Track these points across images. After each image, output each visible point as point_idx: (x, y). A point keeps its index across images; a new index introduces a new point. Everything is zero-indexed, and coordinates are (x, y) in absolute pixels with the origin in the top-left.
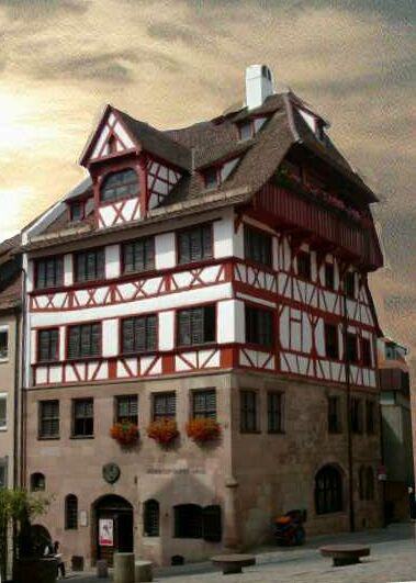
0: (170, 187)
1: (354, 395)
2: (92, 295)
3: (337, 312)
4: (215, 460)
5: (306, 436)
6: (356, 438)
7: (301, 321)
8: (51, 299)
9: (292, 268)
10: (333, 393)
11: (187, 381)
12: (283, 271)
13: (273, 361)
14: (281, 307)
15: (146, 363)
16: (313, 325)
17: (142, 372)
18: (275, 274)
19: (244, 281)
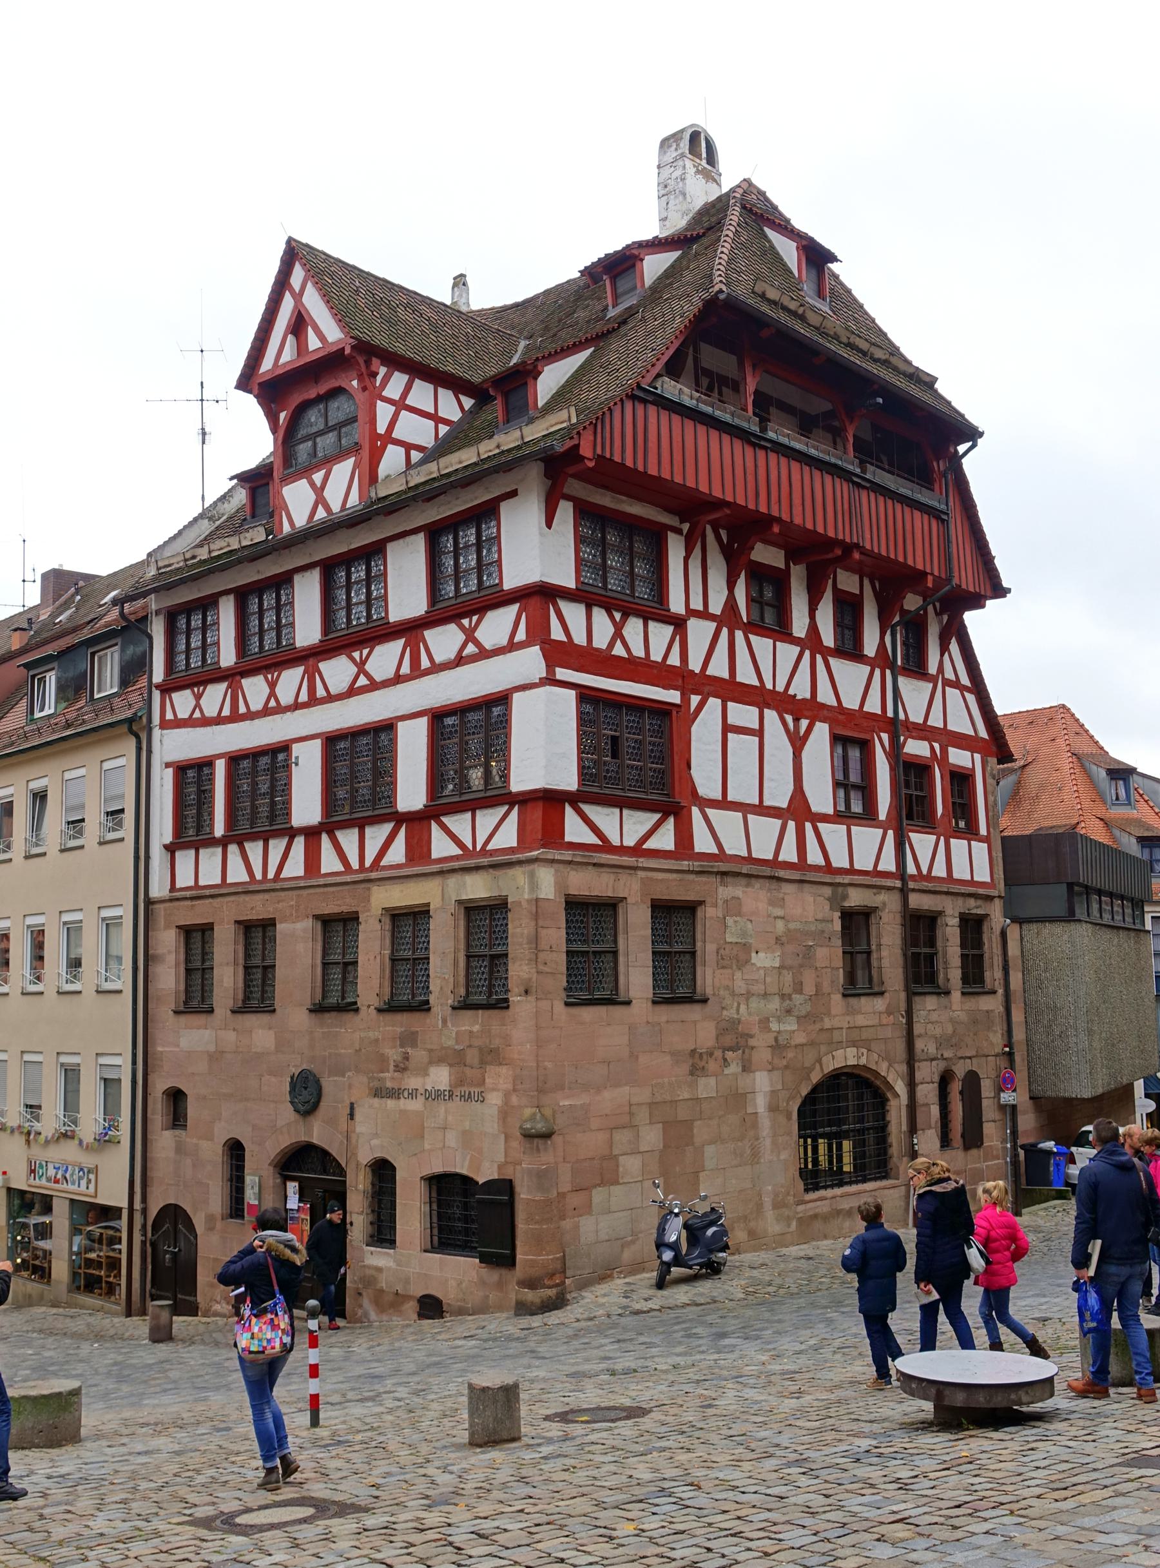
0: (443, 429)
1: (916, 901)
2: (272, 685)
3: (873, 706)
4: (504, 1070)
5: (774, 1004)
6: (927, 1005)
7: (760, 733)
8: (198, 697)
9: (731, 604)
10: (856, 899)
11: (452, 881)
12: (705, 615)
14: (695, 700)
15: (376, 835)
16: (798, 742)
17: (368, 864)
18: (679, 624)
19: (580, 639)
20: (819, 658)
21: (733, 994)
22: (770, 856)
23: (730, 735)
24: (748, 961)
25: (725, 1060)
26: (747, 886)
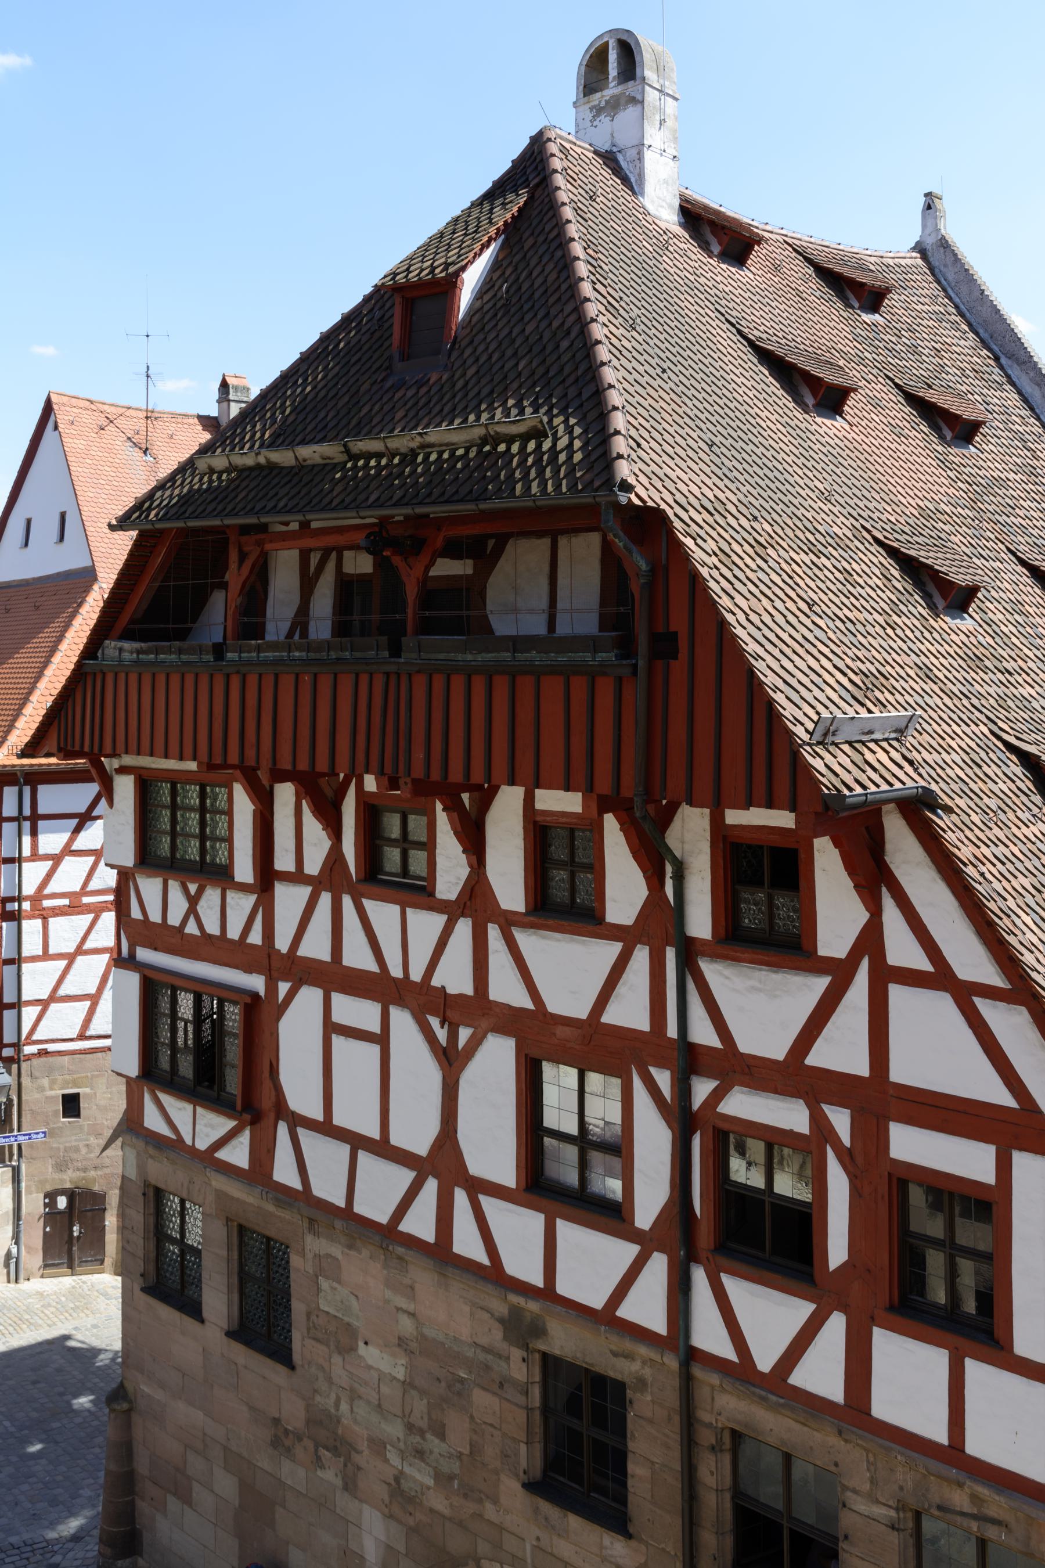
5: (394, 1430)
7: (382, 1039)
9: (335, 856)
12: (298, 877)
13: (245, 1138)
14: (283, 988)
20: (494, 932)
21: (330, 1380)
22: (383, 1218)
23: (335, 1038)
24: (353, 1349)
25: (319, 1458)
26: (350, 1247)
